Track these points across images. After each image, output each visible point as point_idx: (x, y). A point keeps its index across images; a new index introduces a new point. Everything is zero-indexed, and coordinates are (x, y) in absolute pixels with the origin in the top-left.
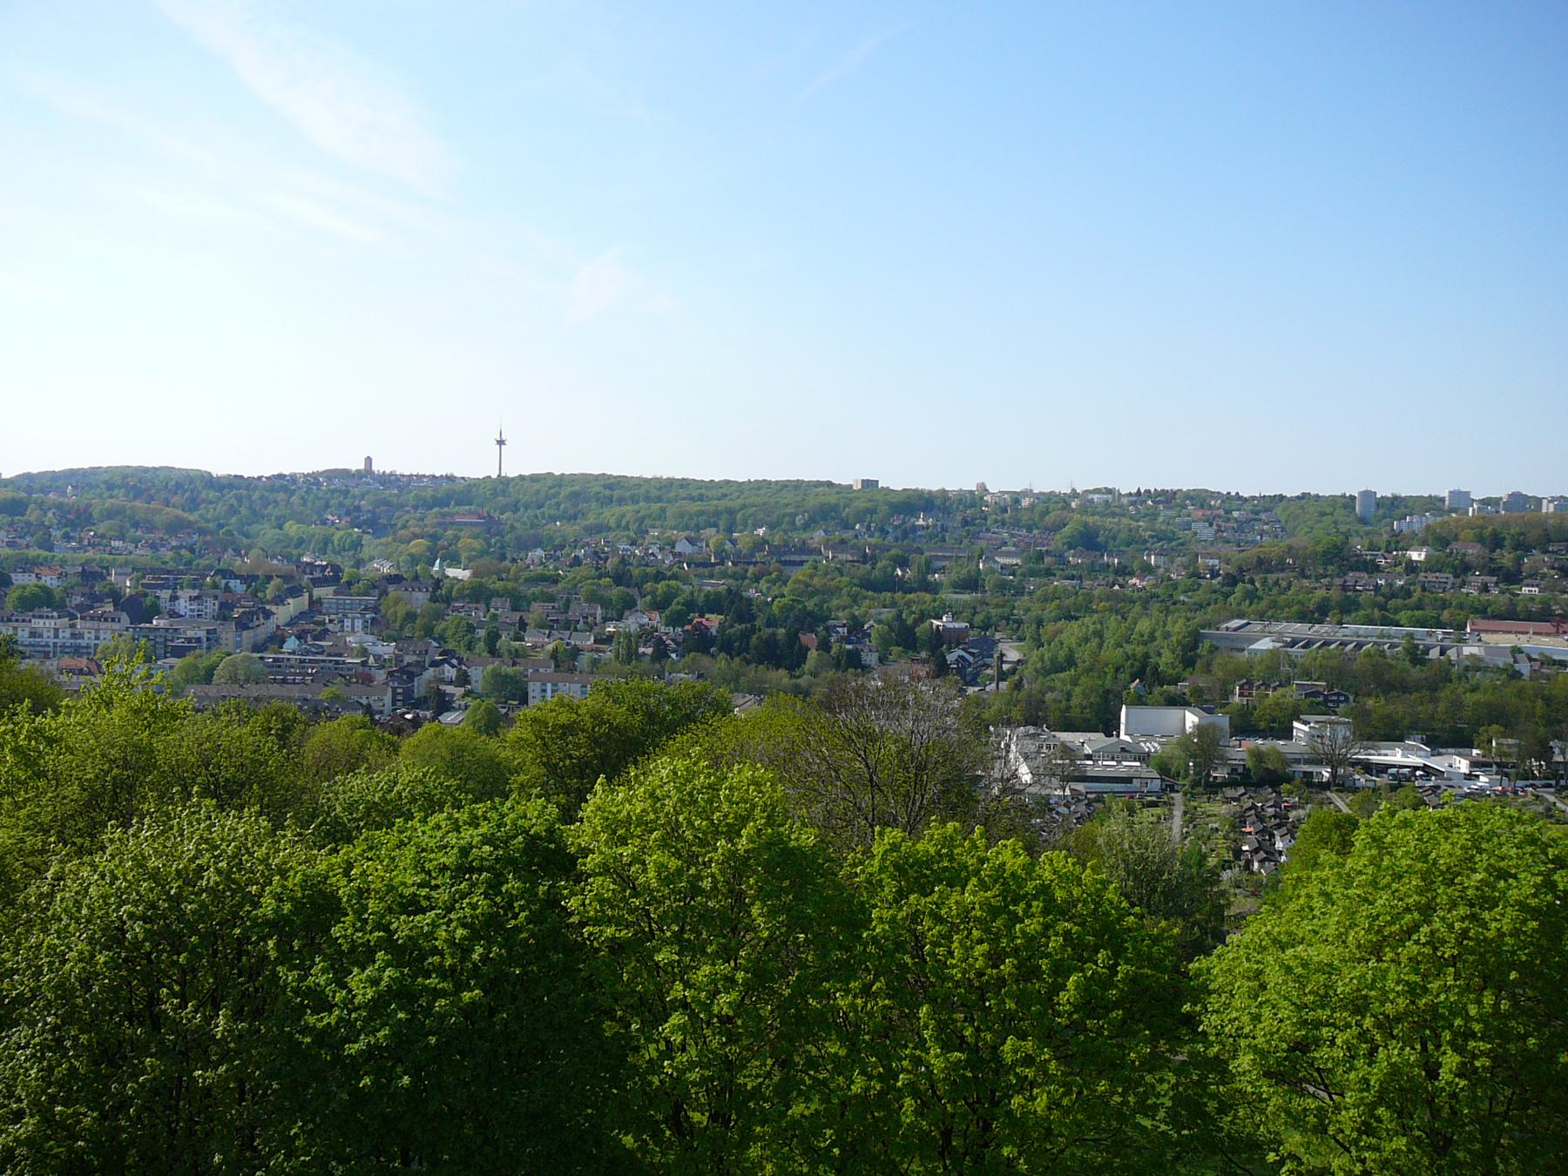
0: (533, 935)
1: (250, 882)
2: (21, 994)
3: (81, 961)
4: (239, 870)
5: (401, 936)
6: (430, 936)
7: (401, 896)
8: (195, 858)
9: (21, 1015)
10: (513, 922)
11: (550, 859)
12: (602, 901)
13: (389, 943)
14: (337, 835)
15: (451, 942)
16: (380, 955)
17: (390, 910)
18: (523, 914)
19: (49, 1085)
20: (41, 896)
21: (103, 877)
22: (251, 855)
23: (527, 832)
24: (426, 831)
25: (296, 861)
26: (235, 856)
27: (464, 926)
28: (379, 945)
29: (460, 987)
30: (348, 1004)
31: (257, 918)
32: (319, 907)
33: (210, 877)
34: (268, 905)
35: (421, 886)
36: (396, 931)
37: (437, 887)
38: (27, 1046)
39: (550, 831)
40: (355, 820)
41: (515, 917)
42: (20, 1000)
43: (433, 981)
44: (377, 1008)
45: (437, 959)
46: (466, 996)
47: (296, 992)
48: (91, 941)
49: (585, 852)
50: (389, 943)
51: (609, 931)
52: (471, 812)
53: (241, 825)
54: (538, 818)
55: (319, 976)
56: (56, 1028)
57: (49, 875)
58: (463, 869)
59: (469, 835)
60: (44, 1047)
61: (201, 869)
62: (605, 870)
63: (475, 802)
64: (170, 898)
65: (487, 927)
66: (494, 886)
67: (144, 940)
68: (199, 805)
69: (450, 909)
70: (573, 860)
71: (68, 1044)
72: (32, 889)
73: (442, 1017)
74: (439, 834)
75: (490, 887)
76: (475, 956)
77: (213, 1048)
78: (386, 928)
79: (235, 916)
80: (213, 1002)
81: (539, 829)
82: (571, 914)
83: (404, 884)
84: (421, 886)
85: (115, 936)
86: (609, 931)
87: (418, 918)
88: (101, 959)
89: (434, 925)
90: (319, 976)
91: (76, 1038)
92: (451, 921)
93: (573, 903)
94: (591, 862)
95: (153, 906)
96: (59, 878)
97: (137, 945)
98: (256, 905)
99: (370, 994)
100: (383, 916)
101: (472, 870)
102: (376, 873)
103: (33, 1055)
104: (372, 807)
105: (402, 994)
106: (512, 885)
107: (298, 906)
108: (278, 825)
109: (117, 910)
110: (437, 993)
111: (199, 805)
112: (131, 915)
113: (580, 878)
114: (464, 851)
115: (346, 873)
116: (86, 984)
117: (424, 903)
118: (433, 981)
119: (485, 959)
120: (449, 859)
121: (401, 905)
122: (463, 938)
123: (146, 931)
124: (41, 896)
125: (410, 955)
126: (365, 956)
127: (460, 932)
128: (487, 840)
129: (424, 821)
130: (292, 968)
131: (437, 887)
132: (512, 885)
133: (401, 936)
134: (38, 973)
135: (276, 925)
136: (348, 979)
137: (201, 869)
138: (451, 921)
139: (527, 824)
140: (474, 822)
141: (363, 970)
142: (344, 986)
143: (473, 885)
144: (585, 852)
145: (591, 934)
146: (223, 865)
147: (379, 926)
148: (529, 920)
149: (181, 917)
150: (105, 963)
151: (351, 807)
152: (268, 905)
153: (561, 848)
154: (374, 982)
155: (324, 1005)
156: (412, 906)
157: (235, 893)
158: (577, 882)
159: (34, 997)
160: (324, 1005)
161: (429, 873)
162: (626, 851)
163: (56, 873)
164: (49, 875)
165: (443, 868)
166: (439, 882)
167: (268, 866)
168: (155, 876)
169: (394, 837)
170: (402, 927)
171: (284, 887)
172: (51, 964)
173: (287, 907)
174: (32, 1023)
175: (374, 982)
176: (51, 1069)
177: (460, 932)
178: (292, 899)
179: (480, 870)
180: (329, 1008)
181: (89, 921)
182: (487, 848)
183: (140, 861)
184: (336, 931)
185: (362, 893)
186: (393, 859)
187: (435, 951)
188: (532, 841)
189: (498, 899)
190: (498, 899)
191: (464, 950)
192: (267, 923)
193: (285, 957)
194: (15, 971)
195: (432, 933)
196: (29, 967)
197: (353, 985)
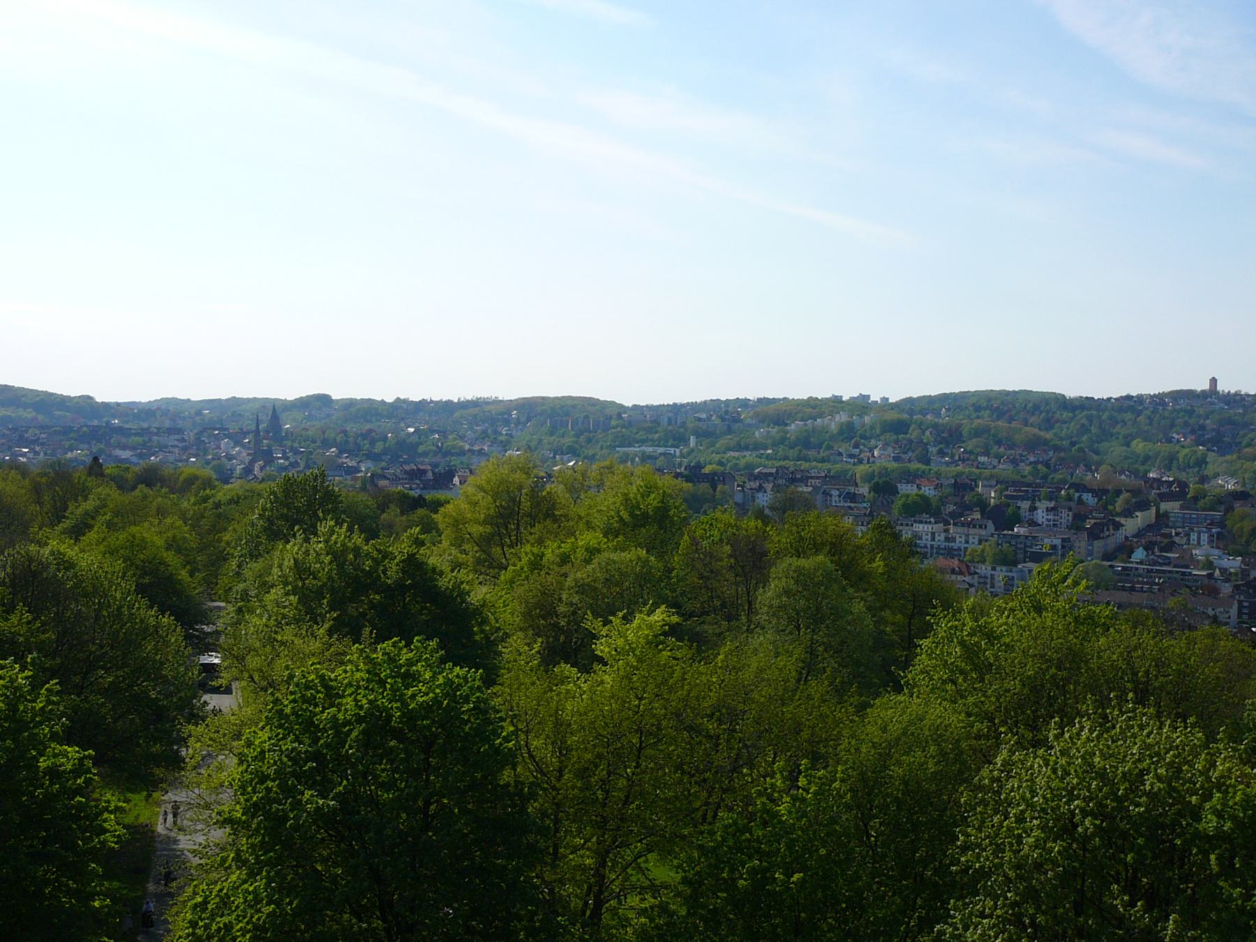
2: (982, 867)
8: (1139, 760)
9: (985, 886)
20: (993, 780)
21: (1054, 771)
22: (1192, 766)
38: (990, 916)
42: (983, 874)
47: (1242, 910)
48: (1043, 828)
56: (1015, 904)
57: (999, 760)
60: (1004, 920)
61: (1142, 773)
64: (1117, 799)
67: (1093, 835)
68: (1134, 710)
72: (985, 772)
80: (1158, 902)
85: (1067, 828)
95: (1101, 805)
97: (1086, 839)
98: (1196, 814)
108: (1211, 738)
109: (1068, 803)
111: (1134, 710)
116: (1038, 866)
123: (1095, 825)
124: (993, 780)
134: (999, 849)
135: (1220, 837)
137: (1142, 773)
146: (1162, 771)
150: (1059, 852)
163: (1004, 760)
164: (999, 760)
167: (1209, 779)
168: (1102, 775)
172: (1011, 844)
174: (995, 898)
194: (979, 845)
196: (991, 844)
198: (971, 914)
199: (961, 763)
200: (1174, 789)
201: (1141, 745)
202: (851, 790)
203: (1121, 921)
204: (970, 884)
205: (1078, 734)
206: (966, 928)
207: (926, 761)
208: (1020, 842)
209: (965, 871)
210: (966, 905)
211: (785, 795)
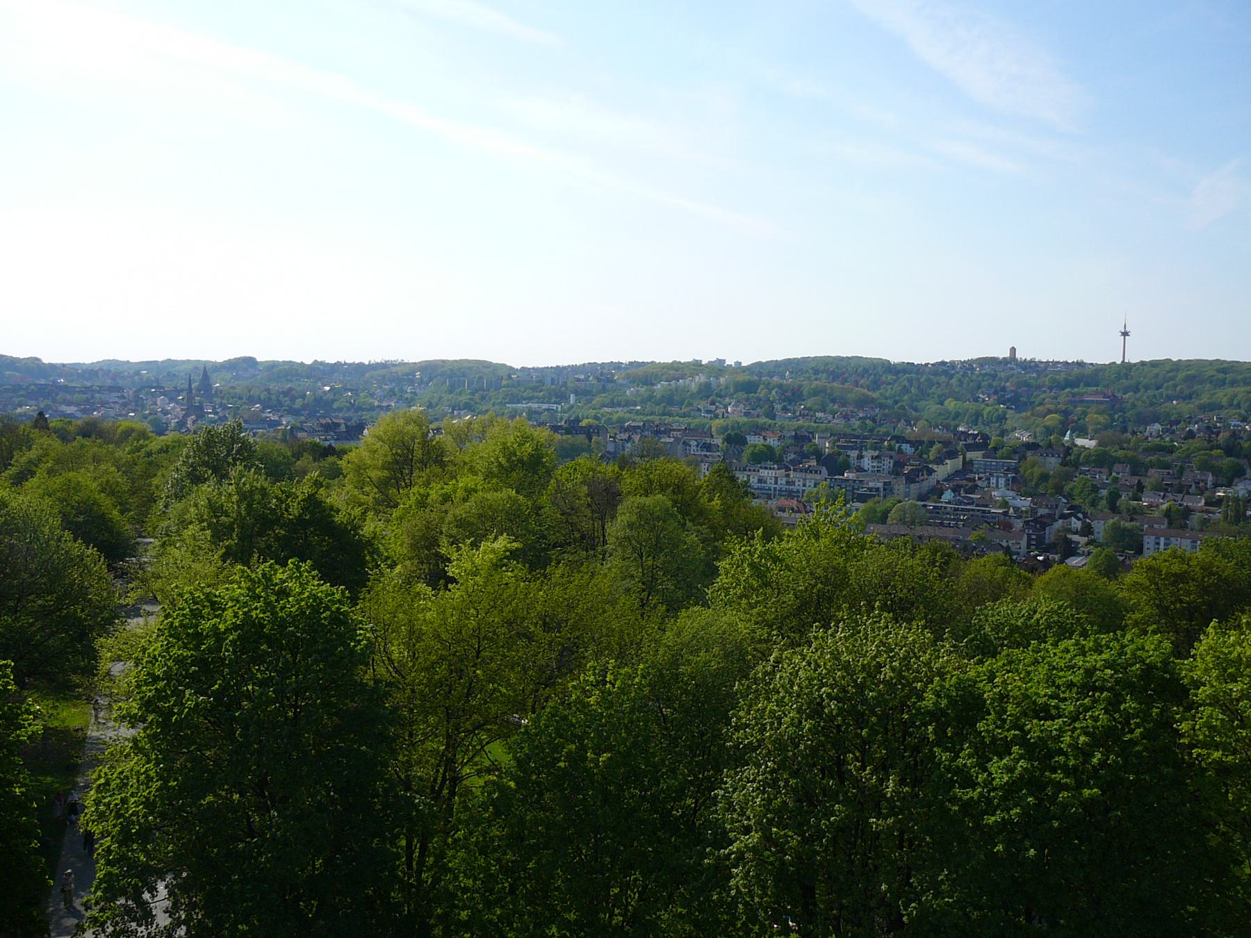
0: (1146, 749)
1: (917, 680)
3: (792, 724)
4: (908, 670)
5: (1034, 736)
6: (1057, 739)
7: (1034, 703)
9: (750, 758)
10: (1129, 736)
11: (1163, 687)
12: (1211, 728)
13: (1023, 741)
14: (986, 650)
15: (1074, 746)
16: (1015, 749)
17: (1024, 714)
18: (1138, 731)
19: (769, 811)
20: (766, 673)
21: (809, 664)
22: (918, 658)
23: (1143, 662)
24: (1059, 653)
25: (950, 666)
26: (905, 658)
27: (1086, 734)
28: (1014, 742)
29: (1080, 785)
30: (988, 782)
31: (920, 708)
32: (967, 706)
33: (886, 673)
34: (929, 700)
35: (1051, 697)
36: (1029, 731)
37: (1065, 699)
39: (1165, 663)
40: (1000, 638)
41: (1132, 731)
42: (751, 748)
43: (1058, 776)
44: (1011, 790)
45: (1062, 759)
46: (1086, 792)
47: (948, 769)
48: (799, 711)
49: (1197, 684)
50: (1023, 741)
51: (1217, 755)
52: (1096, 640)
53: (911, 634)
54: (1155, 650)
55: (966, 759)
56: (773, 771)
57: (772, 658)
58: (1088, 687)
59: (1093, 659)
60: (765, 783)
61: (880, 666)
62: (1214, 701)
63: (1100, 632)
64: (856, 685)
65: (1104, 738)
66: (1113, 706)
67: (838, 715)
69: (1075, 719)
70: (1185, 691)
71: (782, 784)
72: (760, 668)
73: (1065, 806)
74: (1068, 656)
75: (1110, 704)
76: (1095, 760)
77: (884, 804)
78: (1021, 729)
79: (903, 704)
80: (883, 768)
81: (1153, 657)
82: (1182, 736)
83: (1036, 694)
84: (1051, 697)
85: (815, 709)
86: (1217, 755)
87: (1048, 723)
88: (807, 725)
89: (1060, 729)
90: (966, 759)
91: (787, 781)
92: (1075, 728)
93: (1184, 727)
94: (1203, 692)
95: (844, 690)
96: (777, 662)
97: (831, 718)
98: (921, 698)
99: (1006, 779)
100: (1018, 719)
101: (1095, 689)
102: (1015, 684)
103: (758, 788)
104: (1014, 629)
105: (1032, 782)
106: (1130, 704)
107: (952, 702)
108: (939, 638)
109: (818, 690)
110: (1060, 787)
112: (829, 695)
113: (1191, 706)
114: (1089, 672)
115: (991, 677)
117: (1053, 712)
118: (1058, 776)
119: (1103, 764)
120: (1076, 678)
121: (1034, 711)
122: (1086, 744)
124: (766, 673)
125: (1042, 752)
126: (1003, 749)
127: (1082, 739)
128: (1108, 665)
129: (1055, 645)
130: (946, 750)
131: (1065, 699)
132: (1130, 704)
133: (1034, 736)
134: (763, 730)
135: (935, 715)
136: (989, 765)
137: (880, 666)
138: (1075, 728)
139: (1144, 655)
140: (1098, 649)
141: (1002, 759)
142: (985, 770)
143: (1095, 701)
144: (1197, 684)
145: (1199, 755)
147: (1017, 726)
148: (1143, 736)
149: (865, 701)
151: (997, 628)
152: (929, 700)
153: (1175, 680)
154: (1010, 770)
155: (970, 783)
156: (1044, 713)
157: (904, 689)
158: (1188, 709)
159: (759, 746)
160: (970, 783)
161: (1058, 687)
162: (1236, 688)
163: (776, 658)
164: (772, 658)
165: (1071, 685)
166: (1067, 695)
168: (846, 667)
169: (1029, 656)
170: (1035, 729)
171: (943, 687)
173: (944, 702)
174: (758, 766)
175: (1010, 770)
176: (770, 801)
177: (1082, 739)
178: (948, 697)
179: (1102, 689)
180: (973, 785)
181: (798, 696)
182: (1109, 671)
183: (836, 656)
184: (981, 726)
185: (1003, 697)
186: (1029, 673)
187: (1061, 752)
188: (1149, 669)
189: (1117, 716)
190: (1117, 716)
191: (1086, 754)
192: (929, 713)
193: (941, 740)
194: (747, 726)
195: (1060, 736)
196: (757, 724)
197: (993, 770)
198: (741, 780)
199: (739, 660)
200: (904, 678)
201: (875, 643)
202: (649, 685)
203: (857, 782)
204: (739, 758)
205: (833, 636)
206: (735, 790)
207: (710, 660)
208: (780, 724)
209: (736, 747)
210: (737, 774)
211: (591, 685)
